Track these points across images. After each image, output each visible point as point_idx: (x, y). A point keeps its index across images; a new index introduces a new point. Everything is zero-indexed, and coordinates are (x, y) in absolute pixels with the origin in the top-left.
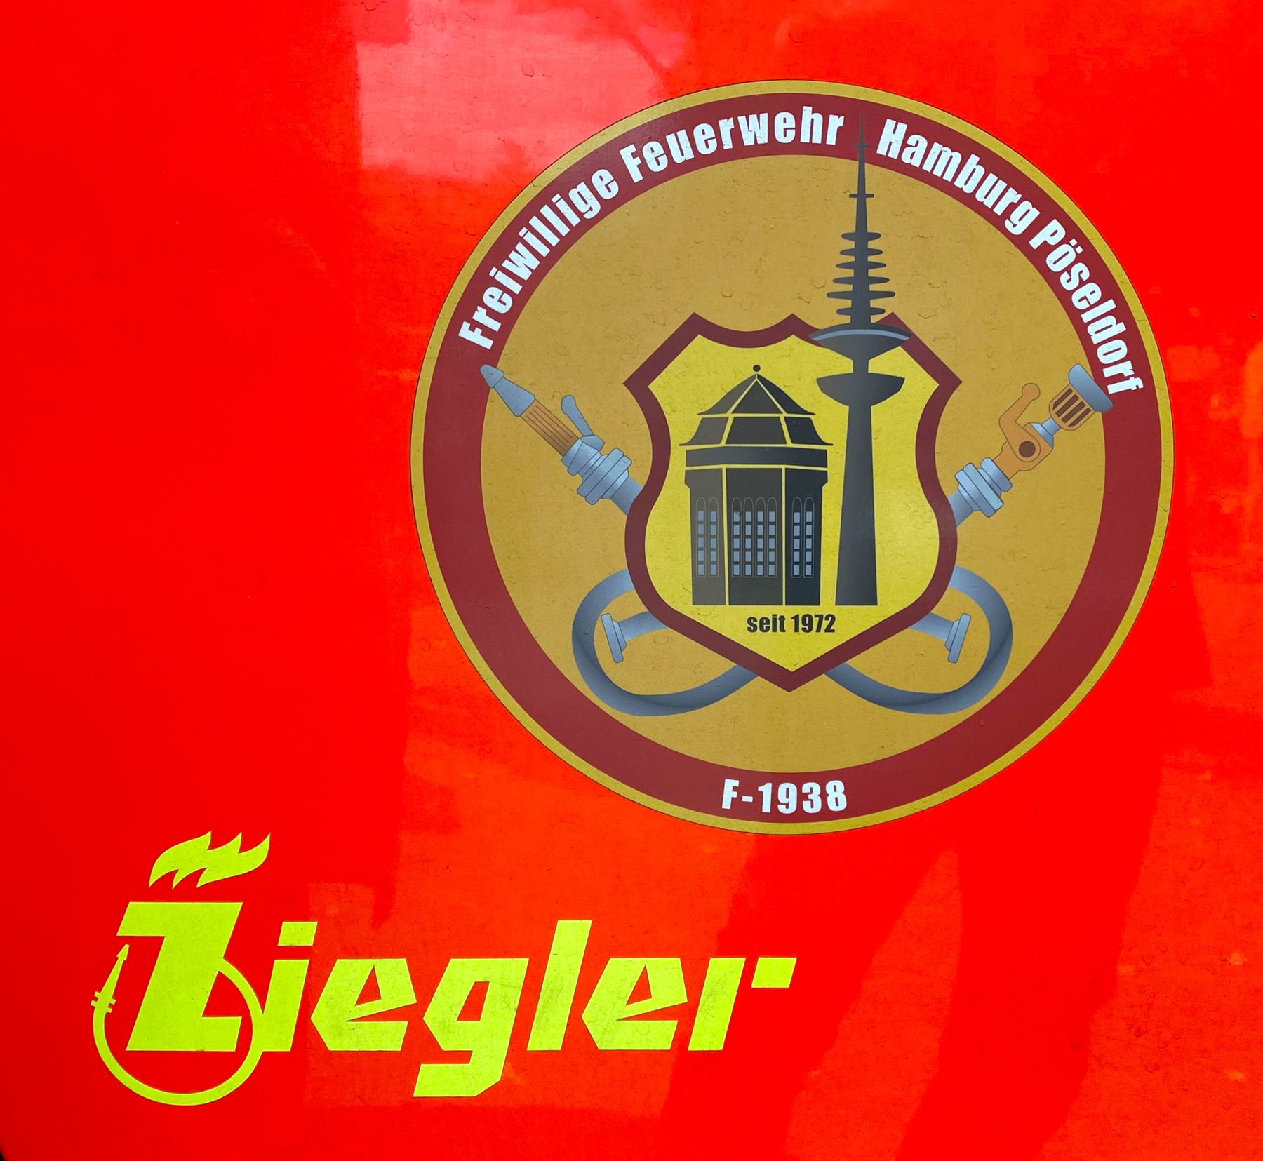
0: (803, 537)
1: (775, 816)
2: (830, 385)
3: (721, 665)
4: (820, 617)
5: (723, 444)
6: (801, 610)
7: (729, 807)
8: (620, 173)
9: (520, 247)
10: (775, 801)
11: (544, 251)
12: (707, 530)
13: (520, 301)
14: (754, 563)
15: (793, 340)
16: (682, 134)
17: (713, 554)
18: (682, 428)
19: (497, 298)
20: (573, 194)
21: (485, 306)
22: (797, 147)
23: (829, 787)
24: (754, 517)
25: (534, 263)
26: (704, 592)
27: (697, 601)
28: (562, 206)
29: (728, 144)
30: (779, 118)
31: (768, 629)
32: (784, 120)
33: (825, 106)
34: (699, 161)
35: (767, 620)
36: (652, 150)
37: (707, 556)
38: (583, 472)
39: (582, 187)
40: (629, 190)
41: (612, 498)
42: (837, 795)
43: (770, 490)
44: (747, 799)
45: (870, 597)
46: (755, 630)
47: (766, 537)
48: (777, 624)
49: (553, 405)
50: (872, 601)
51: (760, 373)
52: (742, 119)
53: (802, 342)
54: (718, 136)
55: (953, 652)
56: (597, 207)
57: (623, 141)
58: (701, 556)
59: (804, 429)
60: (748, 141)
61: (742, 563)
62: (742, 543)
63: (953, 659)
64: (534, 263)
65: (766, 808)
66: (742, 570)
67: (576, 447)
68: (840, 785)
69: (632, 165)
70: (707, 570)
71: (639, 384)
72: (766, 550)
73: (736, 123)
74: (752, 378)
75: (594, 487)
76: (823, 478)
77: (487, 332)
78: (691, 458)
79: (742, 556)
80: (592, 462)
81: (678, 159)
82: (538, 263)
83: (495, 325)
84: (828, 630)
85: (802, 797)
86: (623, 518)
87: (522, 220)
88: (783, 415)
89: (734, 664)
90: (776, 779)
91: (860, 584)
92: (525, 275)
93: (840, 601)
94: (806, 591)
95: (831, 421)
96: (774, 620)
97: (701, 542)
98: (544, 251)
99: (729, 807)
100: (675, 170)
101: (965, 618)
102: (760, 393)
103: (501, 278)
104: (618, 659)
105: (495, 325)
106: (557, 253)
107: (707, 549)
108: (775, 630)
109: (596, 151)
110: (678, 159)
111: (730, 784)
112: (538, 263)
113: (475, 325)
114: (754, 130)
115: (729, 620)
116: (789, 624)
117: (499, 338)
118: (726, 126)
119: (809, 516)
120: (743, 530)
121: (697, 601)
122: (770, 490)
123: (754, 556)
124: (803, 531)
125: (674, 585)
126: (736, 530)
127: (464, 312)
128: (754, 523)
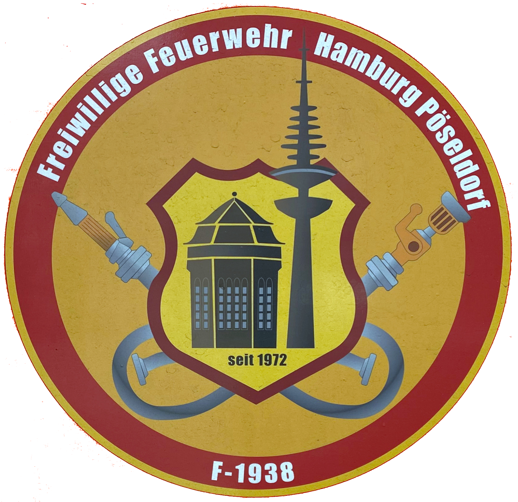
0: (265, 304)
1: (247, 485)
2: (283, 205)
3: (211, 387)
4: (277, 356)
5: (212, 243)
6: (264, 351)
7: (216, 479)
8: (144, 67)
9: (77, 115)
10: (247, 475)
11: (94, 118)
12: (202, 299)
13: (77, 150)
14: (233, 321)
15: (259, 176)
16: (185, 42)
17: (206, 315)
18: (185, 233)
19: (62, 148)
20: (113, 81)
21: (54, 154)
22: (261, 50)
23: (283, 466)
24: (233, 290)
25: (87, 126)
26: (200, 339)
27: (194, 346)
28: (106, 89)
29: (215, 48)
30: (249, 31)
31: (242, 363)
32: (253, 33)
33: (280, 24)
34: (196, 59)
35: (242, 358)
36: (165, 52)
37: (202, 316)
38: (119, 261)
39: (119, 76)
40: (149, 78)
41: (139, 278)
42: (288, 471)
43: (244, 275)
44: (228, 474)
45: (310, 343)
46: (233, 364)
47: (241, 312)
48: (248, 360)
49: (100, 218)
50: (311, 345)
51: (237, 197)
52: (225, 32)
53: (265, 177)
54: (209, 43)
55: (365, 378)
56: (129, 90)
57: (146, 46)
58: (198, 316)
59: (266, 233)
60: (229, 46)
61: (225, 321)
62: (225, 308)
63: (365, 383)
64: (87, 126)
65: (241, 479)
66: (225, 325)
67: (115, 245)
68: (290, 465)
69: (152, 62)
70: (202, 325)
71: (156, 205)
72: (241, 312)
73: (221, 35)
74: (232, 200)
75: (126, 271)
76: (279, 265)
77: (56, 170)
78: (191, 252)
79: (225, 316)
80: (126, 255)
81: (182, 58)
82: (89, 125)
83: (61, 166)
84: (282, 364)
85: (265, 473)
86: (148, 291)
87: (79, 98)
88: (252, 224)
89: (219, 386)
90: (248, 461)
91: (303, 333)
92: (81, 133)
93: (290, 345)
94: (267, 339)
95: (284, 228)
96: (246, 358)
97: (197, 307)
98: (94, 118)
99: (216, 479)
100: (180, 65)
101: (373, 357)
102: (237, 210)
103: (65, 135)
104: (143, 383)
105: (61, 166)
106: (102, 119)
107: (202, 312)
108: (246, 364)
109: (128, 53)
110: (182, 58)
111: (217, 465)
112: (89, 125)
113: (47, 166)
114: (233, 39)
115: (216, 357)
116: (256, 360)
117: (64, 175)
118: (214, 36)
119: (269, 290)
120: (225, 299)
121: (194, 346)
122: (244, 275)
123: (233, 316)
124: (265, 299)
125: (178, 325)
126: (221, 308)
127: (41, 158)
128: (233, 295)
